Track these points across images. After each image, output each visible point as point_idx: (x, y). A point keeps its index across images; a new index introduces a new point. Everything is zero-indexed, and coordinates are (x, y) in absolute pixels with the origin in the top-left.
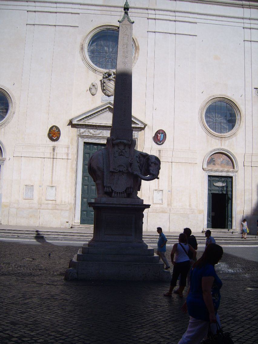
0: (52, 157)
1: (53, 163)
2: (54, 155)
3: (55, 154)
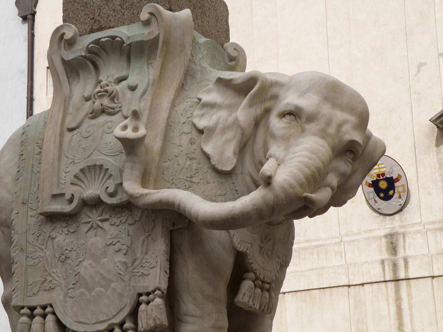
0: (389, 276)
1: (398, 299)
2: (395, 266)
3: (401, 263)
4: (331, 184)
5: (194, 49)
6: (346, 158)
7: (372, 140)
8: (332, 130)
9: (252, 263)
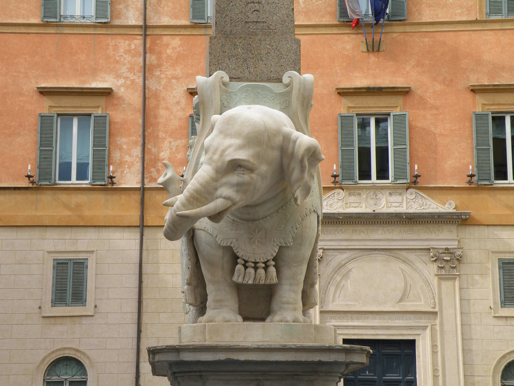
4: (222, 195)
5: (229, 97)
6: (238, 172)
7: (298, 142)
8: (216, 157)
9: (238, 252)
